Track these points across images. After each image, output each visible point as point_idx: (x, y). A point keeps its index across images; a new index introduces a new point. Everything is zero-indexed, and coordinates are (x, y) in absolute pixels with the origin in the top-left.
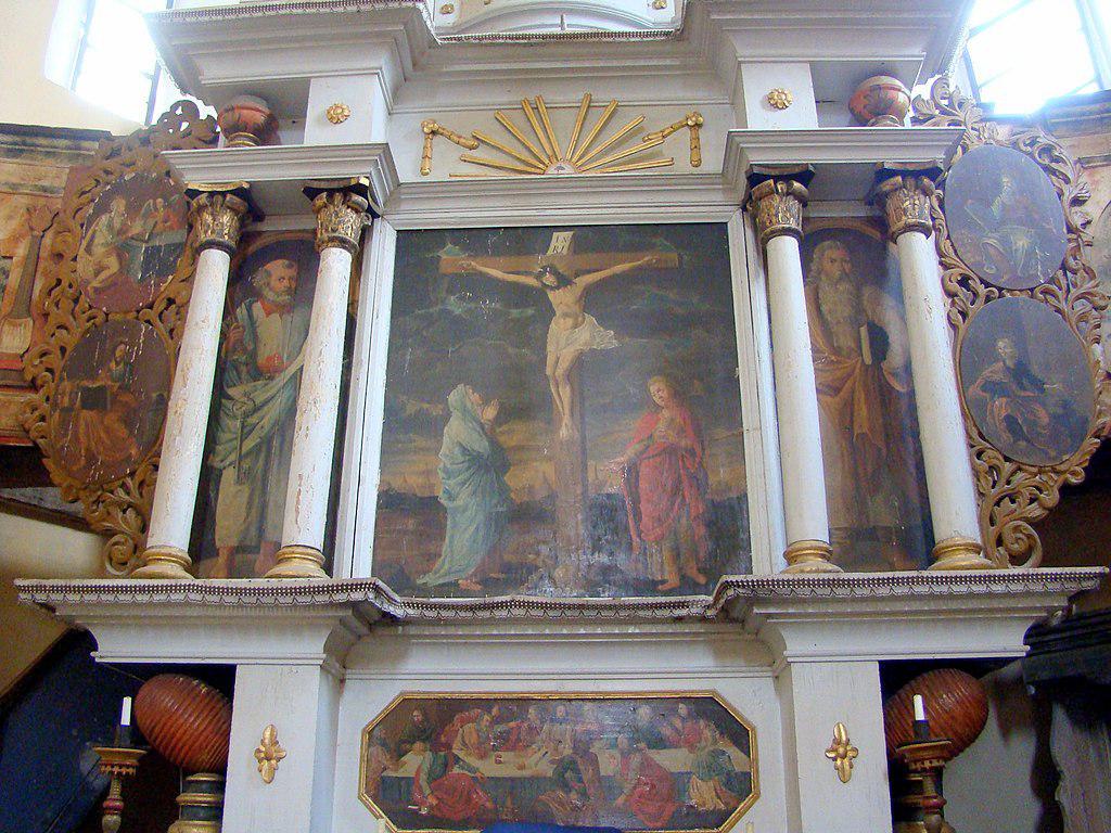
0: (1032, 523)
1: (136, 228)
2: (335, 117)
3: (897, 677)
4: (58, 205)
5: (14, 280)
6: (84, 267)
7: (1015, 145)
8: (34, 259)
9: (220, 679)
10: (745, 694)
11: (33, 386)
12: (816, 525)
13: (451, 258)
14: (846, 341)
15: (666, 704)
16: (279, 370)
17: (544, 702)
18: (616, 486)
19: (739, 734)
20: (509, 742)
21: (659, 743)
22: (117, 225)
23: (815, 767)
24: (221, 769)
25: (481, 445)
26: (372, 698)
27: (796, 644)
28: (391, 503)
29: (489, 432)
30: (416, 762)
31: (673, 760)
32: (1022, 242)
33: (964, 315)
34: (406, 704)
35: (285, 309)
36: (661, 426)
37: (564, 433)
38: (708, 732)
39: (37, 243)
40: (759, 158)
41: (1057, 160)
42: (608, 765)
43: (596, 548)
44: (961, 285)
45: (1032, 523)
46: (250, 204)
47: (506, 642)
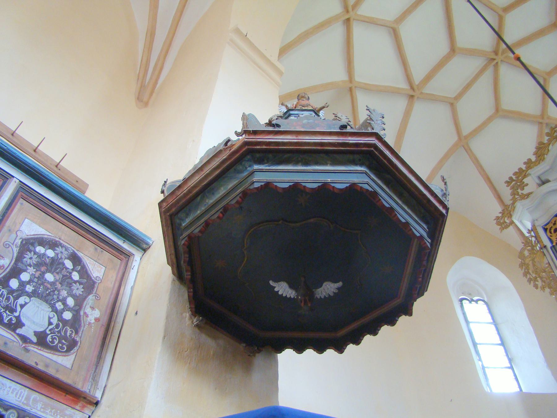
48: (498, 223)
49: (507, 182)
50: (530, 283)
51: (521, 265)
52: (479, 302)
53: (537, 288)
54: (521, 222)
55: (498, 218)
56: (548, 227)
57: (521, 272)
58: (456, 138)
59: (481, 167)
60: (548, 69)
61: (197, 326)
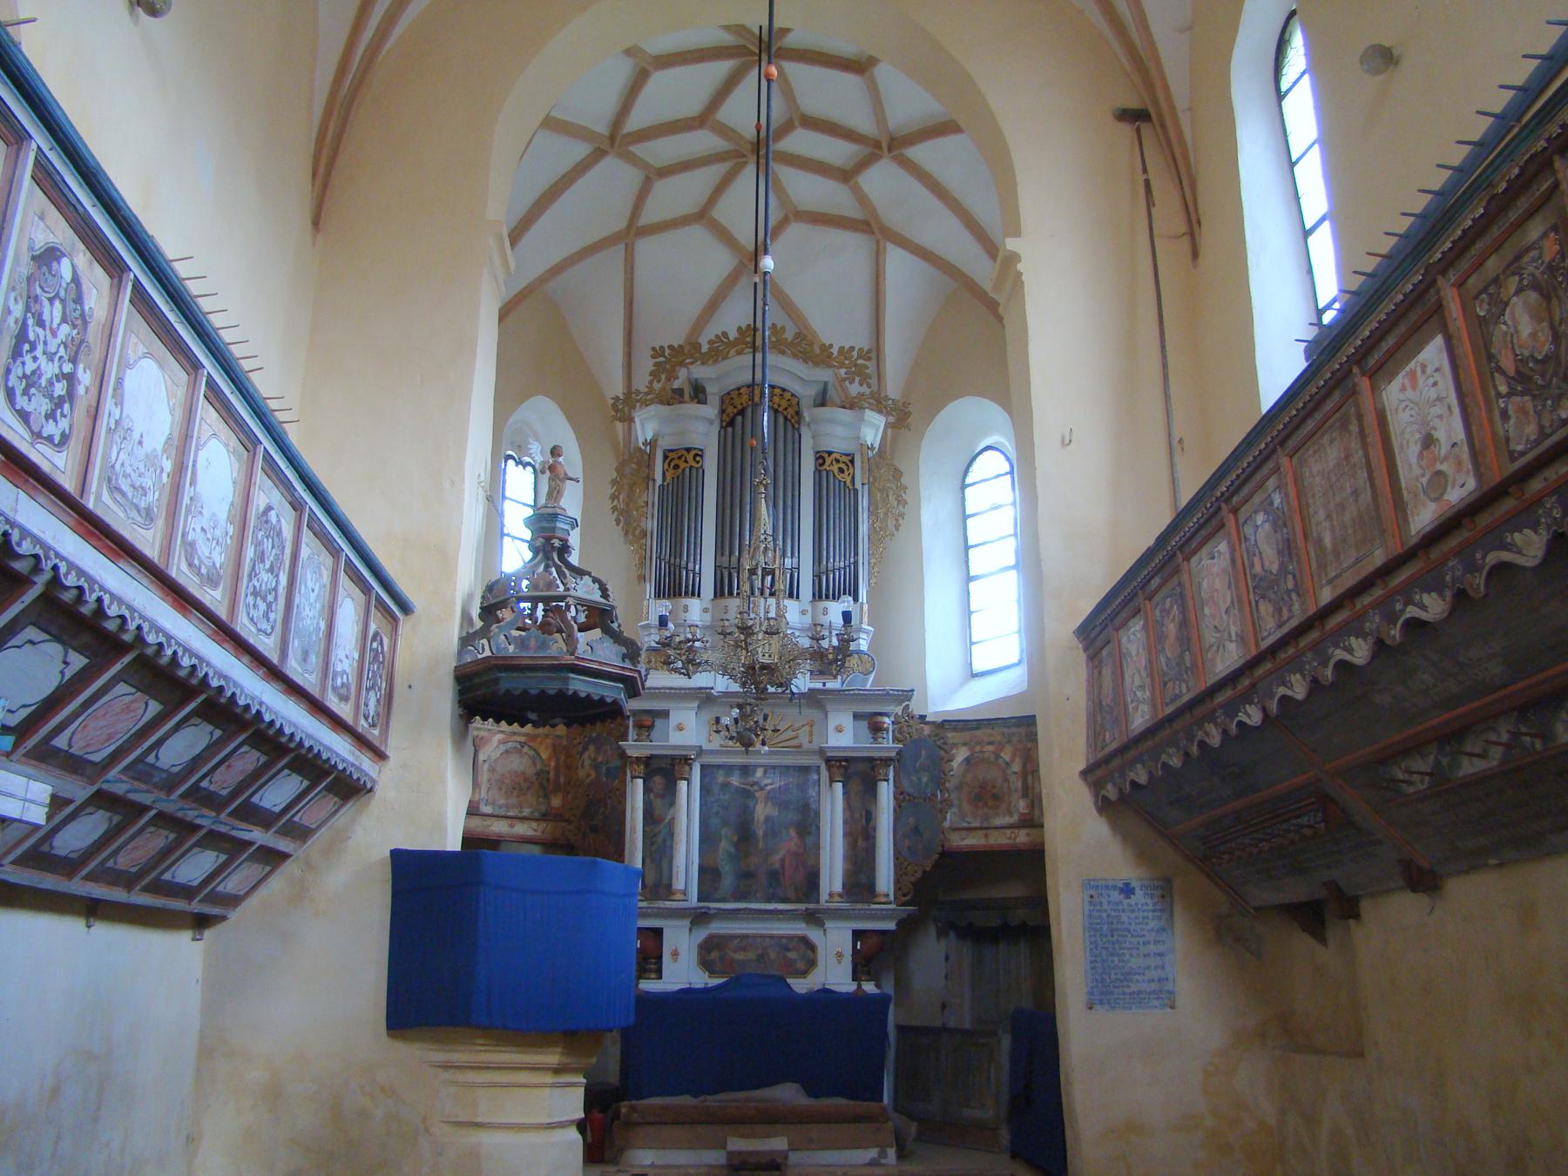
0: (912, 884)
1: (600, 759)
2: (680, 728)
3: (857, 934)
4: (564, 743)
5: (552, 774)
6: (581, 773)
7: (930, 736)
8: (557, 768)
9: (658, 933)
10: (814, 934)
11: (569, 822)
12: (838, 887)
13: (720, 777)
14: (857, 816)
15: (791, 938)
16: (663, 820)
17: (754, 937)
18: (777, 866)
19: (811, 946)
20: (744, 949)
21: (787, 949)
22: (593, 756)
23: (833, 960)
24: (660, 958)
25: (732, 850)
26: (702, 934)
27: (828, 924)
28: (702, 870)
29: (737, 845)
30: (714, 955)
31: (792, 955)
32: (925, 779)
33: (900, 807)
34: (711, 937)
35: (663, 796)
36: (793, 844)
37: (761, 845)
38: (802, 947)
39: (558, 759)
40: (829, 754)
41: (945, 743)
42: (773, 955)
43: (771, 886)
44: (900, 795)
45: (912, 884)
46: (648, 761)
47: (743, 919)
48: (614, 406)
49: (654, 349)
50: (613, 512)
51: (614, 482)
52: (529, 469)
53: (618, 524)
54: (643, 425)
55: (617, 399)
56: (671, 455)
57: (610, 491)
58: (623, 224)
59: (632, 280)
60: (801, 208)
61: (461, 716)
